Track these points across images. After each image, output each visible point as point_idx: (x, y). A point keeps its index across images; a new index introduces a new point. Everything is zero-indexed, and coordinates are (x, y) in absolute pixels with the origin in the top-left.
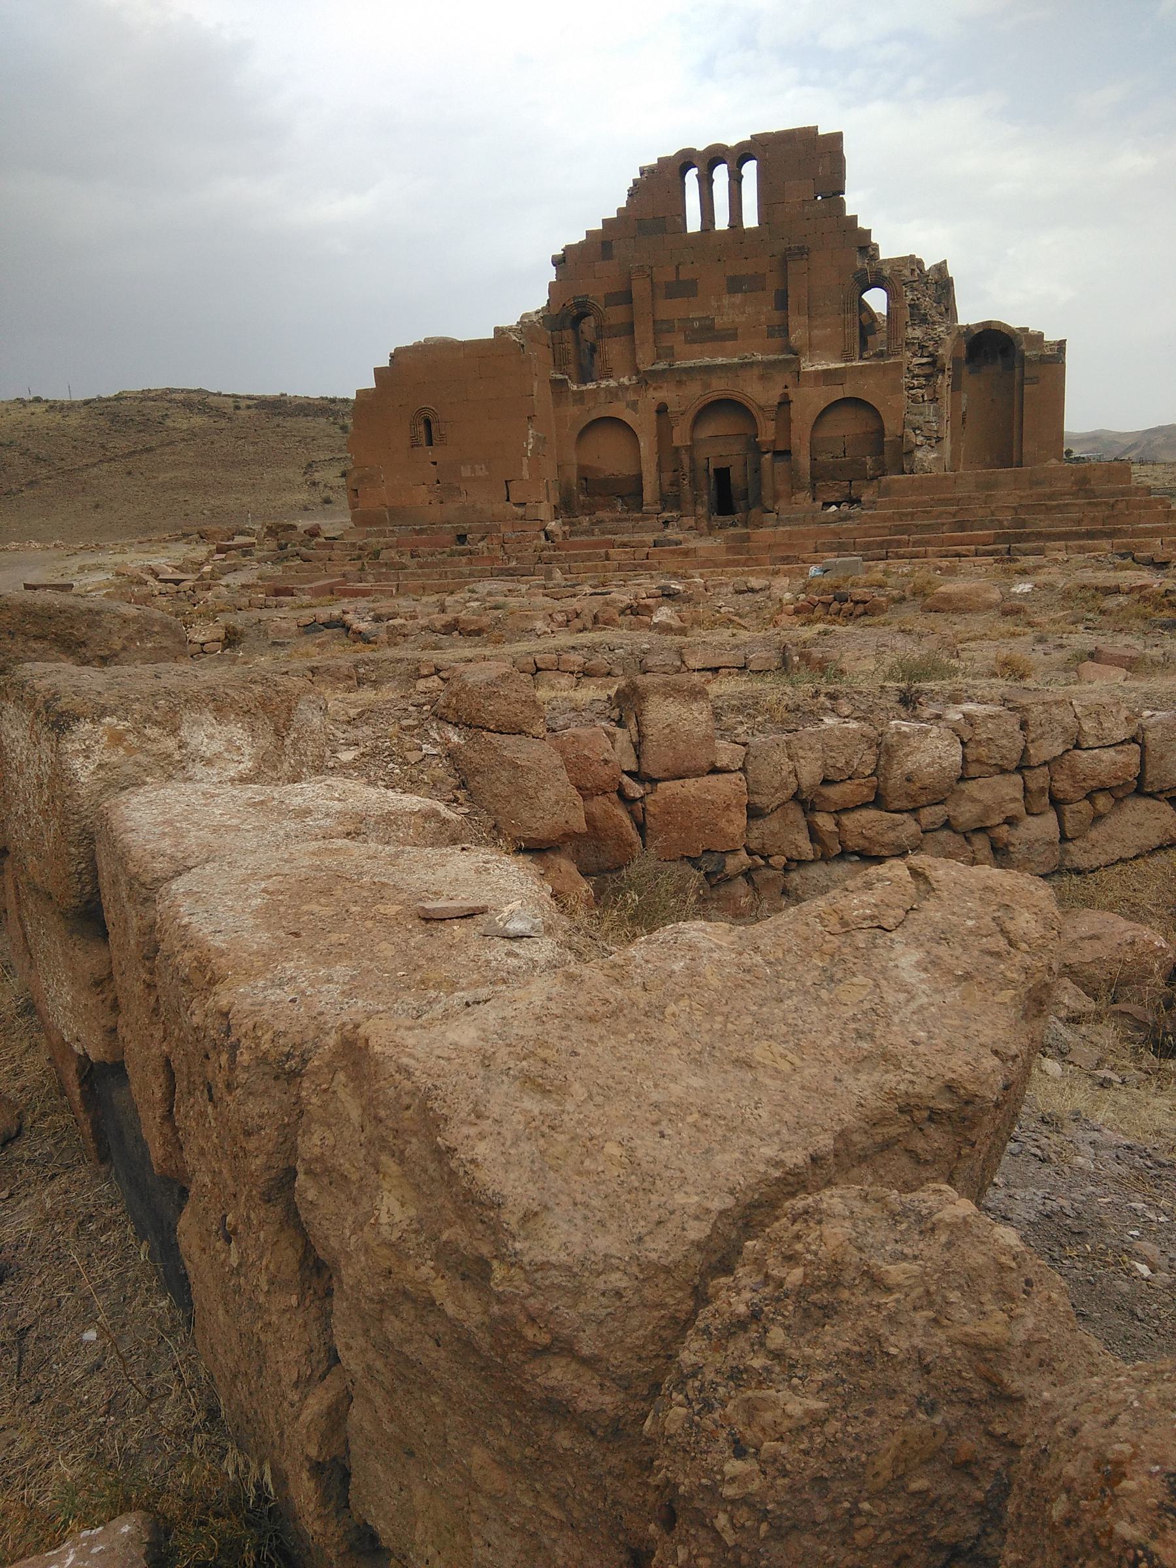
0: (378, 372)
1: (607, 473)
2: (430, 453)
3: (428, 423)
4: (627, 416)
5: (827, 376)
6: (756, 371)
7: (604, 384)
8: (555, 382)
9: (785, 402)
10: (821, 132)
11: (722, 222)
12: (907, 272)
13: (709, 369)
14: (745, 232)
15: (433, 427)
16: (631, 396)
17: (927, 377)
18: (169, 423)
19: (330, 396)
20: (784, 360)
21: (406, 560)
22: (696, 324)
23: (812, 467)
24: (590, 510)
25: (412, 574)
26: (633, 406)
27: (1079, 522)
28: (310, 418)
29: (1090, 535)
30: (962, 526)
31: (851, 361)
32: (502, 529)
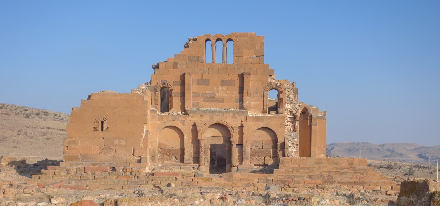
2: (102, 134)
3: (102, 123)
4: (180, 126)
5: (257, 119)
6: (231, 115)
7: (171, 113)
8: (152, 111)
9: (242, 127)
10: (257, 35)
13: (213, 112)
15: (104, 124)
16: (182, 119)
22: (208, 95)
23: (251, 151)
26: (183, 122)
27: (352, 178)
29: (355, 183)
30: (310, 177)
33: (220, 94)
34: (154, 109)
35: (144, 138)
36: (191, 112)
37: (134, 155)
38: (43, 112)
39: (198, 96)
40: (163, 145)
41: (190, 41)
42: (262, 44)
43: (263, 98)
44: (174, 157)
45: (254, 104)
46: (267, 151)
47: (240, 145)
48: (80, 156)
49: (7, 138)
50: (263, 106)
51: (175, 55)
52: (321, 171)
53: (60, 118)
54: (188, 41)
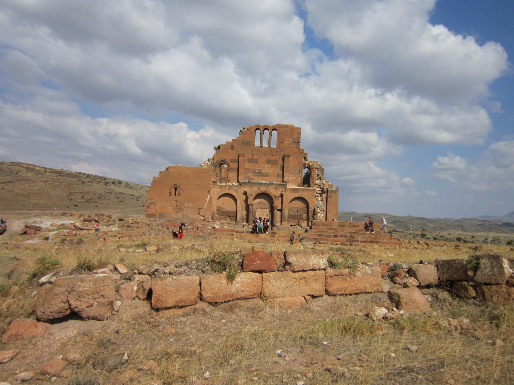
0: (161, 173)
1: (226, 210)
3: (176, 189)
4: (234, 194)
5: (294, 190)
6: (274, 186)
7: (228, 184)
10: (296, 126)
12: (316, 165)
14: (272, 148)
15: (177, 190)
17: (320, 194)
18: (20, 174)
19: (79, 171)
20: (282, 184)
21: (164, 229)
22: (257, 171)
24: (219, 220)
25: (168, 234)
26: (237, 191)
27: (368, 238)
28: (71, 178)
32: (197, 223)
33: (265, 171)
34: (215, 180)
36: (244, 183)
37: (200, 215)
38: (118, 181)
40: (221, 208)
42: (299, 133)
44: (229, 218)
46: (300, 215)
47: (281, 210)
49: (90, 200)
52: (344, 232)
53: (130, 186)
54: (242, 129)
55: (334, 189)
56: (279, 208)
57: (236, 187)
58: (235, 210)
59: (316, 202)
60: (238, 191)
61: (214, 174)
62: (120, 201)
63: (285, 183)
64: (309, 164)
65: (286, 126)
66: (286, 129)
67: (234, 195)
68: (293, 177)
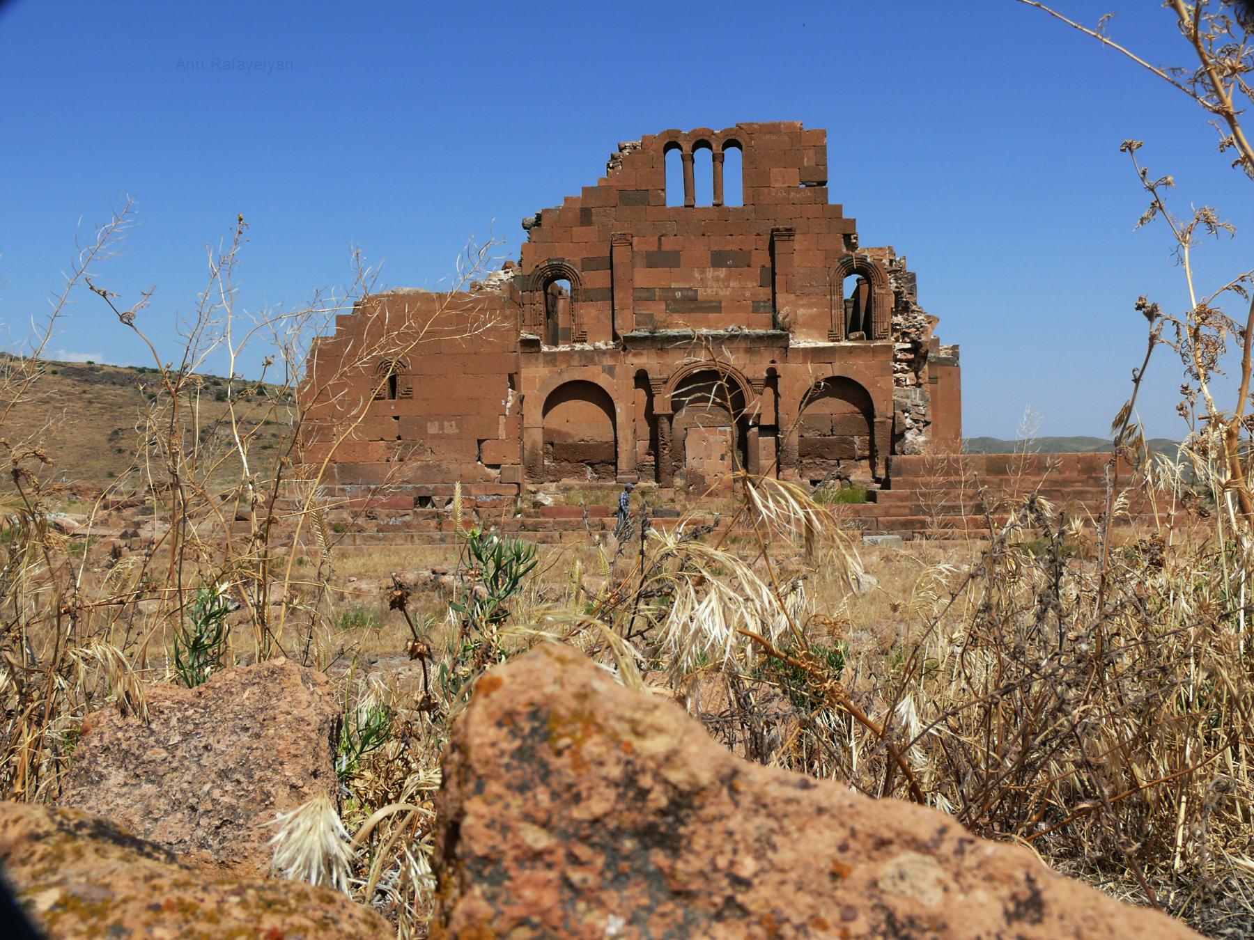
1: (577, 439)
4: (603, 381)
5: (815, 354)
7: (578, 347)
11: (704, 198)
14: (728, 210)
17: (909, 362)
20: (774, 336)
22: (678, 295)
23: (800, 443)
25: (372, 537)
26: (610, 371)
31: (839, 341)
33: (709, 291)
35: (507, 413)
39: (651, 299)
40: (559, 433)
41: (621, 150)
42: (821, 151)
43: (829, 297)
45: (804, 314)
46: (844, 441)
48: (335, 470)
50: (829, 320)
51: (585, 190)
54: (617, 152)
55: (942, 355)
56: (767, 420)
57: (607, 356)
58: (610, 438)
59: (897, 394)
60: (617, 369)
61: (527, 316)
62: (265, 448)
63: (783, 329)
64: (863, 259)
65: (773, 129)
66: (774, 137)
67: (602, 385)
68: (810, 306)
